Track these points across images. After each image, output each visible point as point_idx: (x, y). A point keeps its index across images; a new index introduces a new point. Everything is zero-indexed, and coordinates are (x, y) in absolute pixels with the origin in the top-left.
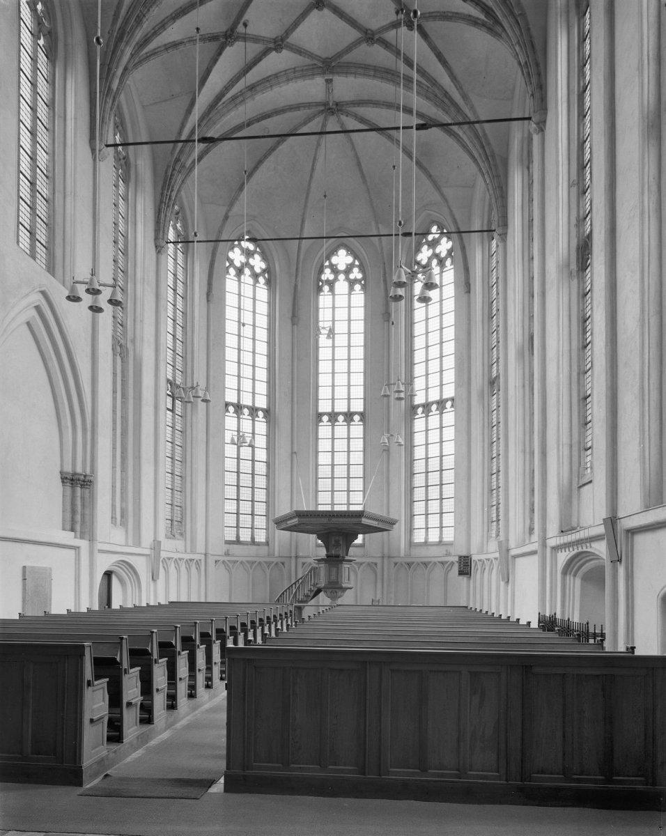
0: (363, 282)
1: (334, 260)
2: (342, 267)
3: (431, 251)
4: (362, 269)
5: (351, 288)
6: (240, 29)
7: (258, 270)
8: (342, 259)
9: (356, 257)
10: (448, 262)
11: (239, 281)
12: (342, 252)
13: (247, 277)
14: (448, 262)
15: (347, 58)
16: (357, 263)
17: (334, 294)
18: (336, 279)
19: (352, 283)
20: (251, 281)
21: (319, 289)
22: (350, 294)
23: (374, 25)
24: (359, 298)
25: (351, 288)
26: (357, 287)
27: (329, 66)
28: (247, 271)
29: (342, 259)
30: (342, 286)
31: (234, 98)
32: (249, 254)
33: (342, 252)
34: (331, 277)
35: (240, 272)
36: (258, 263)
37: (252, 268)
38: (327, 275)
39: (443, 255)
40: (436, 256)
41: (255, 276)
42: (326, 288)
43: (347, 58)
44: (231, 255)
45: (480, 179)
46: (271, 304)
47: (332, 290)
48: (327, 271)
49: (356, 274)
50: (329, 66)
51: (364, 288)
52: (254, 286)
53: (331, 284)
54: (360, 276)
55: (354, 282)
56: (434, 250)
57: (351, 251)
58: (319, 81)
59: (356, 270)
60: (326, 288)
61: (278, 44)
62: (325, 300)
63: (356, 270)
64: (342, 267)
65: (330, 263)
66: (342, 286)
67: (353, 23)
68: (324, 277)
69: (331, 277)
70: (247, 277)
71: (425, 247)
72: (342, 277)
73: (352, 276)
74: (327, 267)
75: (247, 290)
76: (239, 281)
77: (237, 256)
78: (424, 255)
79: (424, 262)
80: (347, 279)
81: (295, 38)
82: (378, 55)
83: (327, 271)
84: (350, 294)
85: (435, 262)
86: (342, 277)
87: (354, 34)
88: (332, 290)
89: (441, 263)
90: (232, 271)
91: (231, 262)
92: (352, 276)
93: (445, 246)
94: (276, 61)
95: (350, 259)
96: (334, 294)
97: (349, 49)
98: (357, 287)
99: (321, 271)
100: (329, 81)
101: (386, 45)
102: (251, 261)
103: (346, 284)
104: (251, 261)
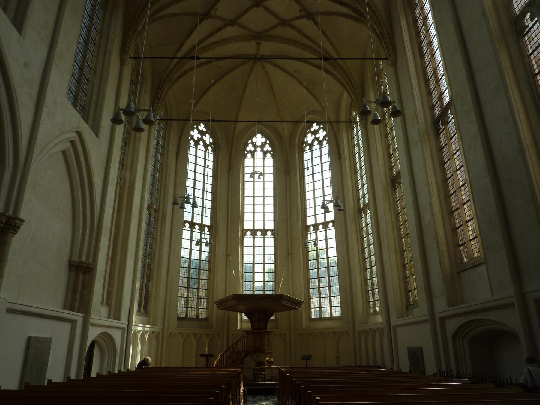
0: (272, 152)
1: (254, 140)
2: (259, 144)
3: (313, 137)
4: (271, 145)
5: (265, 156)
6: (213, 13)
7: (208, 143)
8: (259, 139)
9: (267, 138)
10: (325, 142)
11: (196, 148)
12: (259, 136)
13: (201, 147)
14: (325, 142)
15: (270, 33)
16: (268, 142)
17: (254, 159)
18: (255, 150)
19: (265, 153)
20: (203, 149)
21: (245, 156)
22: (264, 159)
23: (287, 17)
24: (269, 161)
25: (265, 156)
26: (269, 155)
27: (259, 36)
28: (201, 143)
29: (259, 139)
30: (259, 154)
31: (204, 48)
32: (201, 133)
33: (259, 136)
34: (253, 149)
35: (197, 143)
36: (208, 139)
37: (204, 141)
38: (250, 148)
39: (321, 138)
40: (316, 139)
41: (206, 146)
42: (249, 155)
43: (270, 33)
44: (192, 133)
45: (346, 95)
46: (215, 162)
47: (253, 156)
48: (250, 145)
49: (267, 148)
50: (259, 36)
51: (272, 156)
52: (205, 152)
53: (253, 153)
54: (270, 149)
55: (268, 152)
56: (315, 136)
57: (264, 135)
58: (253, 43)
59: (267, 146)
60: (249, 155)
61: (233, 22)
62: (248, 161)
63: (267, 146)
64: (259, 144)
65: (252, 141)
66: (259, 154)
67: (275, 16)
68: (248, 149)
69: (253, 149)
70: (201, 147)
71: (309, 135)
72: (259, 149)
73: (265, 149)
74: (250, 143)
75: (201, 154)
76: (196, 148)
77: (195, 134)
78: (309, 138)
79: (310, 142)
80: (262, 150)
81: (243, 20)
82: (289, 33)
83: (250, 145)
84: (264, 159)
85: (316, 142)
86: (259, 149)
87: (275, 21)
88: (253, 156)
89: (320, 143)
90: (192, 142)
91: (192, 137)
92: (265, 149)
93: (322, 134)
94: (230, 31)
95: (264, 140)
96: (254, 159)
97: (272, 28)
98: (269, 155)
99: (247, 145)
100: (258, 44)
101: (293, 27)
102: (204, 137)
103: (262, 153)
104: (204, 137)
